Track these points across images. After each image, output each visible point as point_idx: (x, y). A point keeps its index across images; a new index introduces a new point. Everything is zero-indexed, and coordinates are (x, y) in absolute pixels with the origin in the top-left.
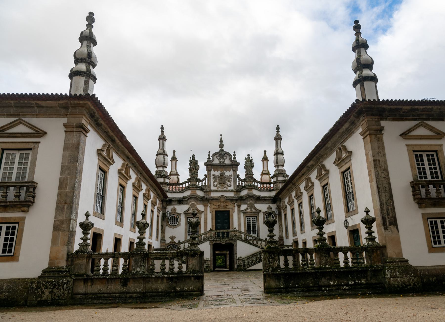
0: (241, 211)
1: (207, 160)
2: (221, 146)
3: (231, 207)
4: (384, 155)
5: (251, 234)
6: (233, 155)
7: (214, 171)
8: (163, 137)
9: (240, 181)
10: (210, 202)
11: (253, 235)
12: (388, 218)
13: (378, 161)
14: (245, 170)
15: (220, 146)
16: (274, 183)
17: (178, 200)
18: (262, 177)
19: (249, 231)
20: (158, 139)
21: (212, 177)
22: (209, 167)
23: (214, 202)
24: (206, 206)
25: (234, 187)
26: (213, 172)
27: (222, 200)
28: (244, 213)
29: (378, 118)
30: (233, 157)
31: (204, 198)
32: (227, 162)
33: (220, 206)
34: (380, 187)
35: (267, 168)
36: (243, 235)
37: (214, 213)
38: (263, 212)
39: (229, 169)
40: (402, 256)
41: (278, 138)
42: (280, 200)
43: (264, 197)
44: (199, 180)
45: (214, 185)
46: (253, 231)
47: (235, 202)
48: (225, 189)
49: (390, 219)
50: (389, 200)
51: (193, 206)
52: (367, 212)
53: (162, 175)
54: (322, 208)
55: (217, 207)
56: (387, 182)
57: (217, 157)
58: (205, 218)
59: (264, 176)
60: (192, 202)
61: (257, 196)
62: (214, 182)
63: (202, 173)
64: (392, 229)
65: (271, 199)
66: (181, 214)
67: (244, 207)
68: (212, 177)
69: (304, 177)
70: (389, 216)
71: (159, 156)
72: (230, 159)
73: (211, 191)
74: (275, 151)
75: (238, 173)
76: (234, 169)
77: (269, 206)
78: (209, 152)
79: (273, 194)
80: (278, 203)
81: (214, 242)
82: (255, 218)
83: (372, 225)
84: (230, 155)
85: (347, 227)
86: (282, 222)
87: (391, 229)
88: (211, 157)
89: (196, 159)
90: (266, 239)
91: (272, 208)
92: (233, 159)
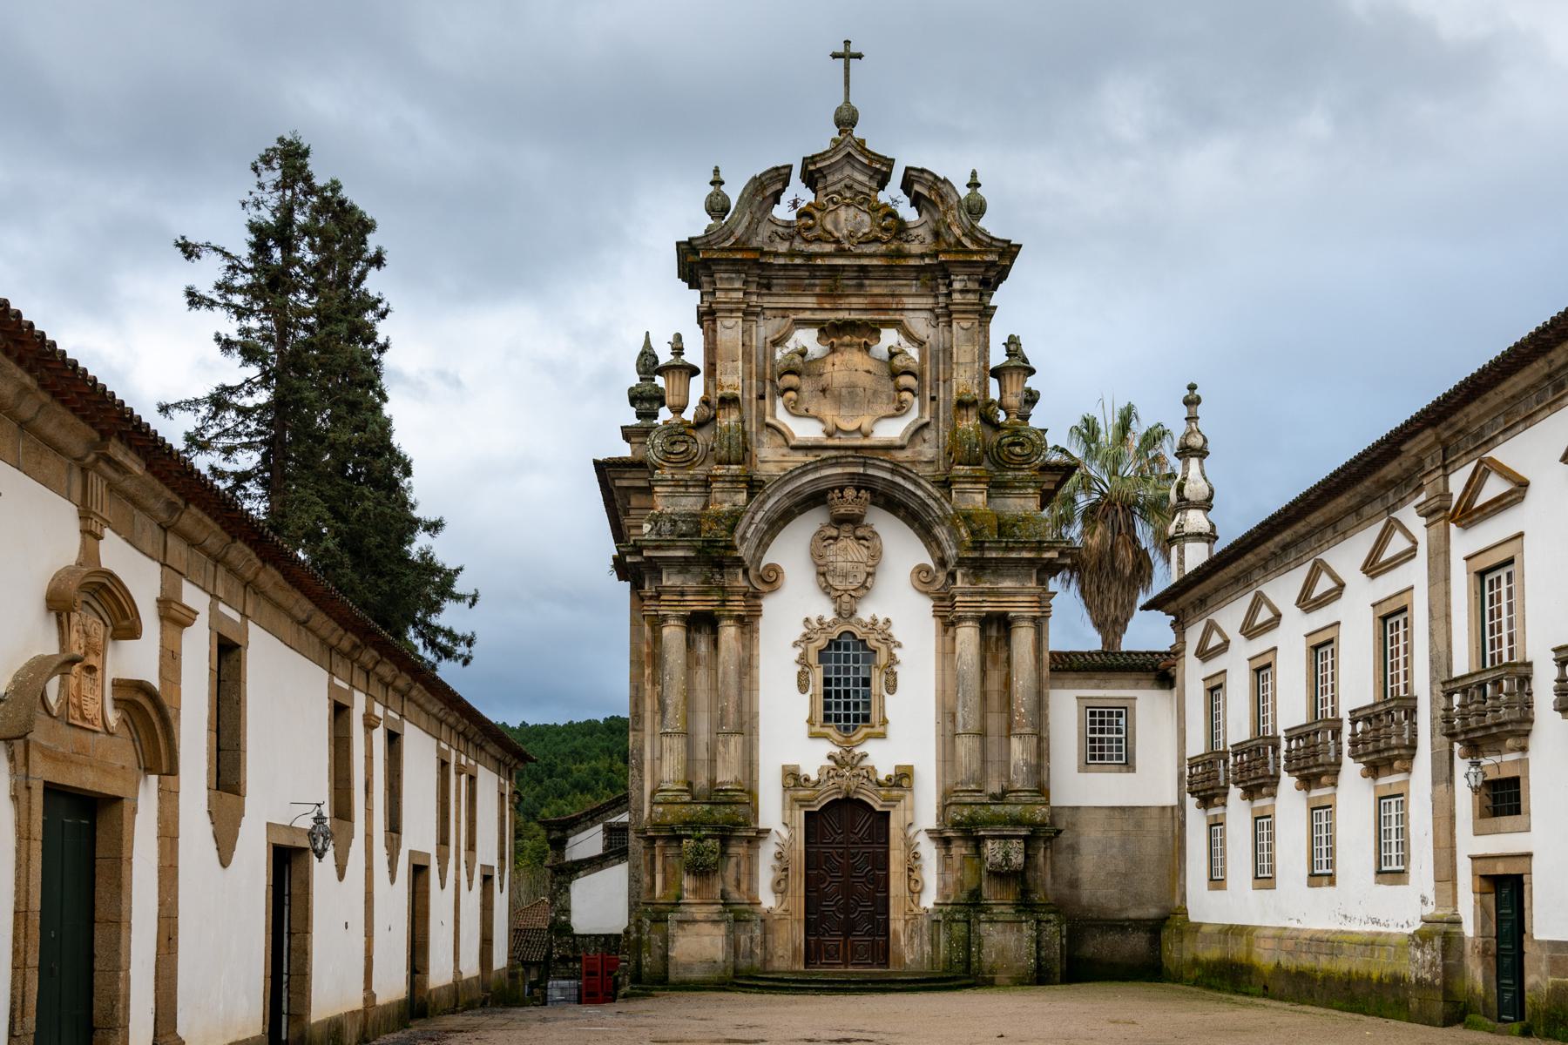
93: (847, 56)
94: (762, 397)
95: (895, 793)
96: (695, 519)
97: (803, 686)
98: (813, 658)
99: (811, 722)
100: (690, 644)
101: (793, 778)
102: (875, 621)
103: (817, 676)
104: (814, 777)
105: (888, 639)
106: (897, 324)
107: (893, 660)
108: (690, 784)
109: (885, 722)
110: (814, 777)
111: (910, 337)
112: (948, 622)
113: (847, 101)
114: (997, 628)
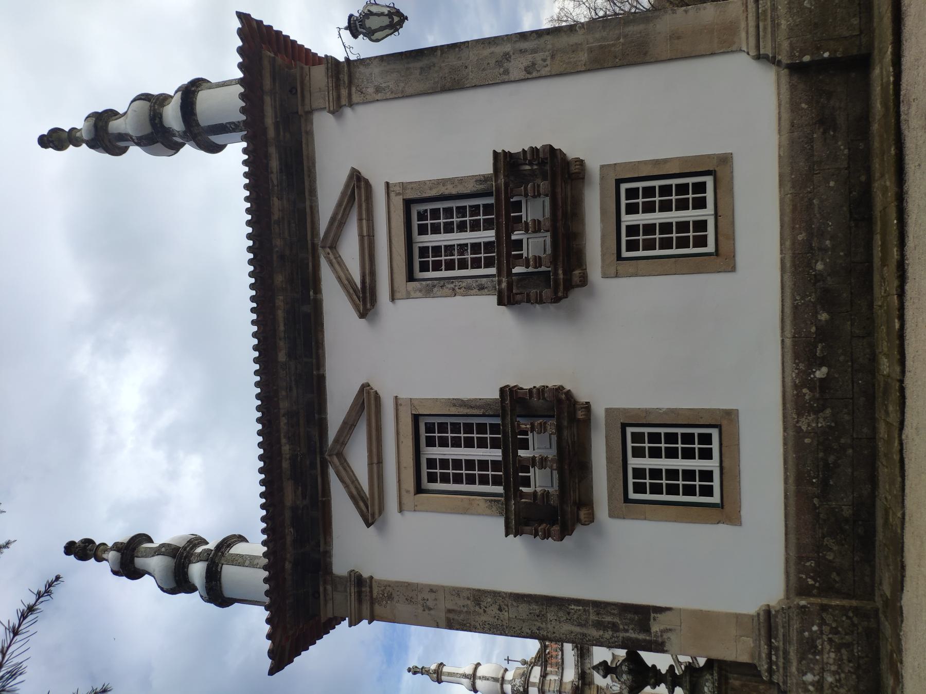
4: (432, 590)
8: (434, 673)
12: (626, 631)
13: (451, 616)
17: (581, 658)
20: (439, 683)
29: (325, 583)
34: (529, 632)
40: (752, 617)
49: (631, 626)
50: (569, 613)
53: (521, 689)
56: (515, 604)
64: (662, 628)
66: (613, 654)
70: (621, 627)
83: (650, 665)
87: (663, 631)
113: (519, 662)
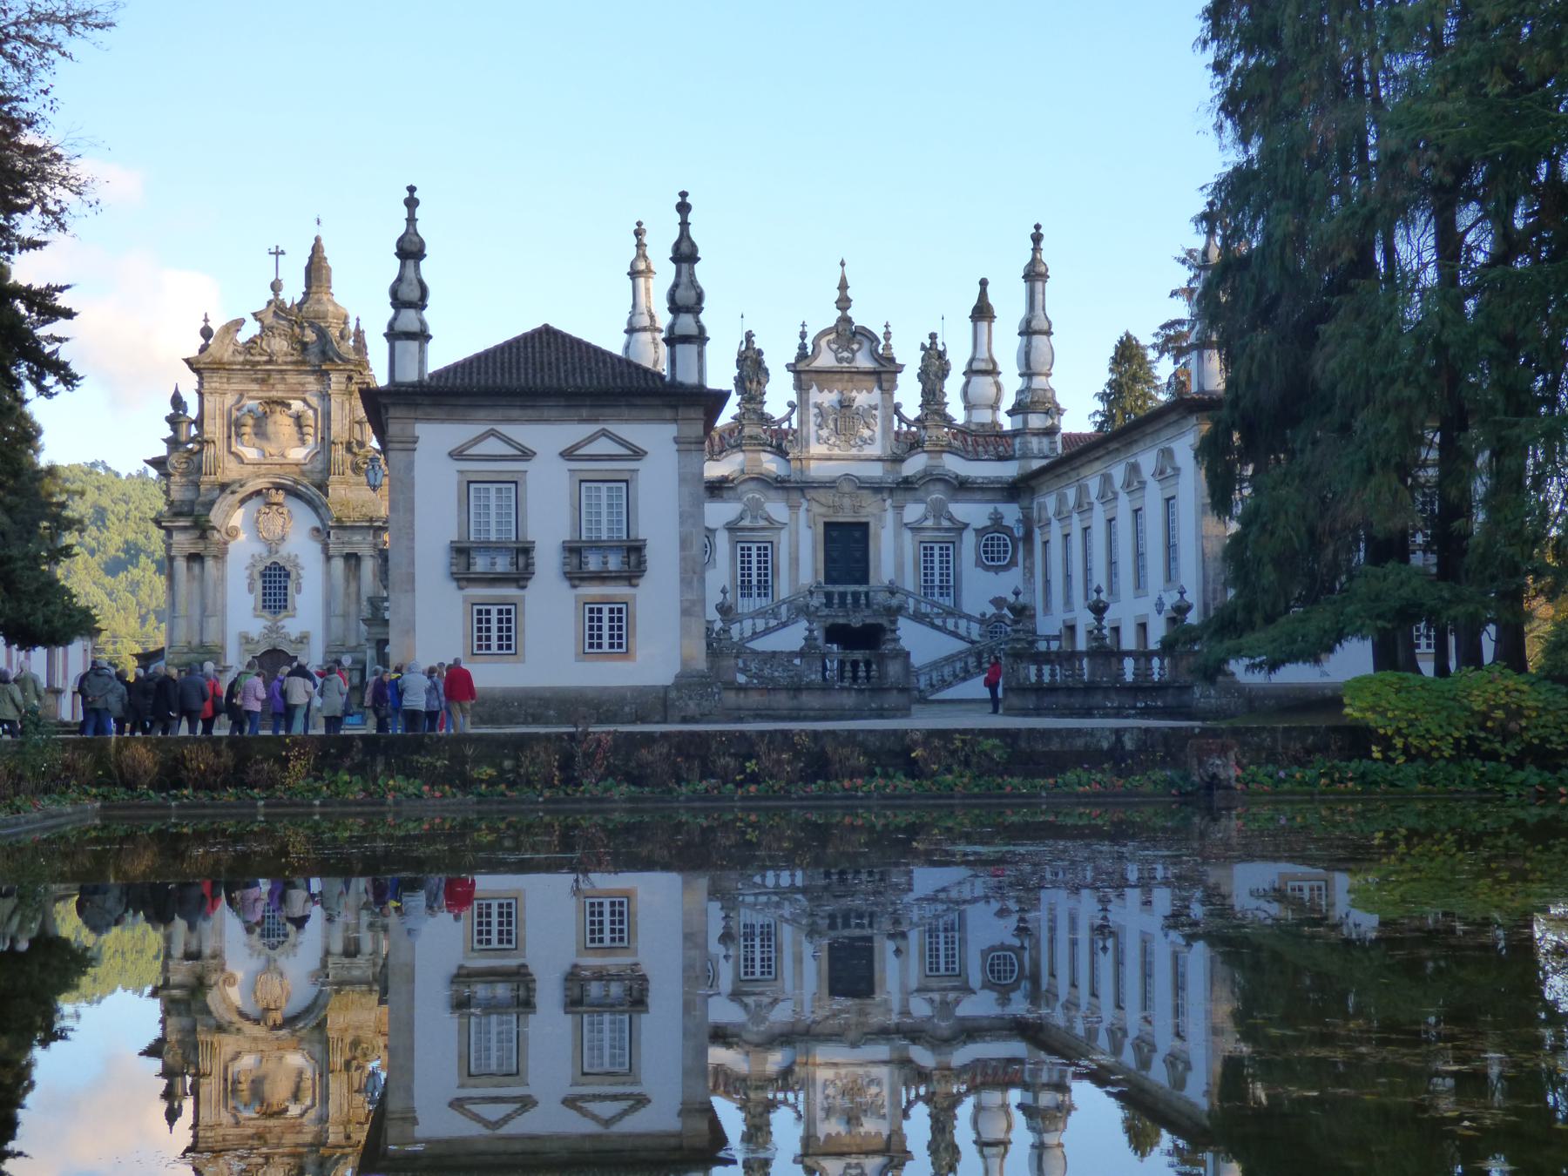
0: (906, 524)
1: (795, 351)
2: (844, 303)
3: (875, 512)
5: (935, 598)
6: (881, 337)
7: (821, 390)
9: (904, 427)
10: (811, 494)
11: (941, 600)
14: (919, 386)
15: (841, 305)
16: (1015, 434)
18: (967, 384)
19: (928, 586)
21: (813, 411)
22: (803, 377)
23: (821, 495)
24: (793, 507)
25: (884, 447)
26: (816, 396)
27: (846, 487)
28: (912, 529)
30: (883, 342)
31: (789, 481)
32: (863, 362)
33: (842, 507)
35: (989, 349)
36: (911, 601)
37: (821, 529)
38: (976, 530)
39: (869, 384)
41: (1034, 274)
42: (1032, 492)
43: (980, 481)
44: (765, 419)
45: (819, 439)
46: (941, 588)
47: (885, 495)
48: (854, 451)
51: (754, 508)
52: (1182, 593)
54: (1104, 586)
55: (831, 510)
57: (829, 342)
58: (790, 547)
59: (976, 380)
60: (752, 493)
61: (957, 477)
62: (820, 426)
63: (779, 396)
65: (1002, 489)
67: (913, 512)
68: (813, 411)
69: (1097, 466)
71: (637, 335)
72: (874, 354)
73: (809, 459)
74: (1024, 323)
75: (898, 397)
76: (885, 385)
77: (996, 509)
78: (803, 325)
79: (1009, 470)
80: (1026, 503)
81: (830, 621)
82: (948, 549)
84: (872, 338)
85: (1159, 612)
86: (1033, 564)
88: (809, 341)
89: (757, 346)
90: (983, 615)
91: (1005, 514)
92: (881, 351)
93: (278, 253)
94: (229, 437)
95: (300, 646)
96: (192, 503)
97: (251, 590)
98: (257, 576)
99: (255, 609)
100: (189, 569)
101: (246, 640)
102: (289, 556)
103: (259, 584)
104: (256, 638)
105: (296, 566)
106: (304, 401)
107: (299, 576)
108: (189, 643)
109: (295, 609)
110: (256, 638)
111: (310, 406)
112: (328, 558)
114: (353, 559)
